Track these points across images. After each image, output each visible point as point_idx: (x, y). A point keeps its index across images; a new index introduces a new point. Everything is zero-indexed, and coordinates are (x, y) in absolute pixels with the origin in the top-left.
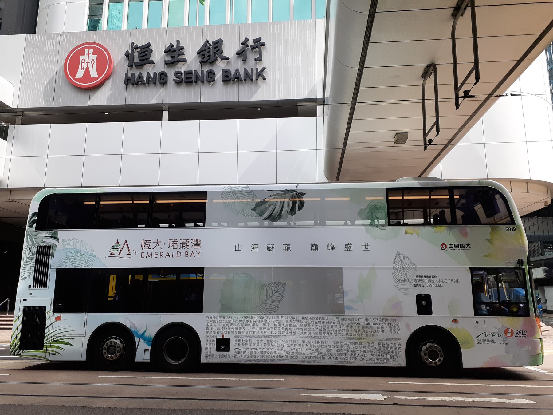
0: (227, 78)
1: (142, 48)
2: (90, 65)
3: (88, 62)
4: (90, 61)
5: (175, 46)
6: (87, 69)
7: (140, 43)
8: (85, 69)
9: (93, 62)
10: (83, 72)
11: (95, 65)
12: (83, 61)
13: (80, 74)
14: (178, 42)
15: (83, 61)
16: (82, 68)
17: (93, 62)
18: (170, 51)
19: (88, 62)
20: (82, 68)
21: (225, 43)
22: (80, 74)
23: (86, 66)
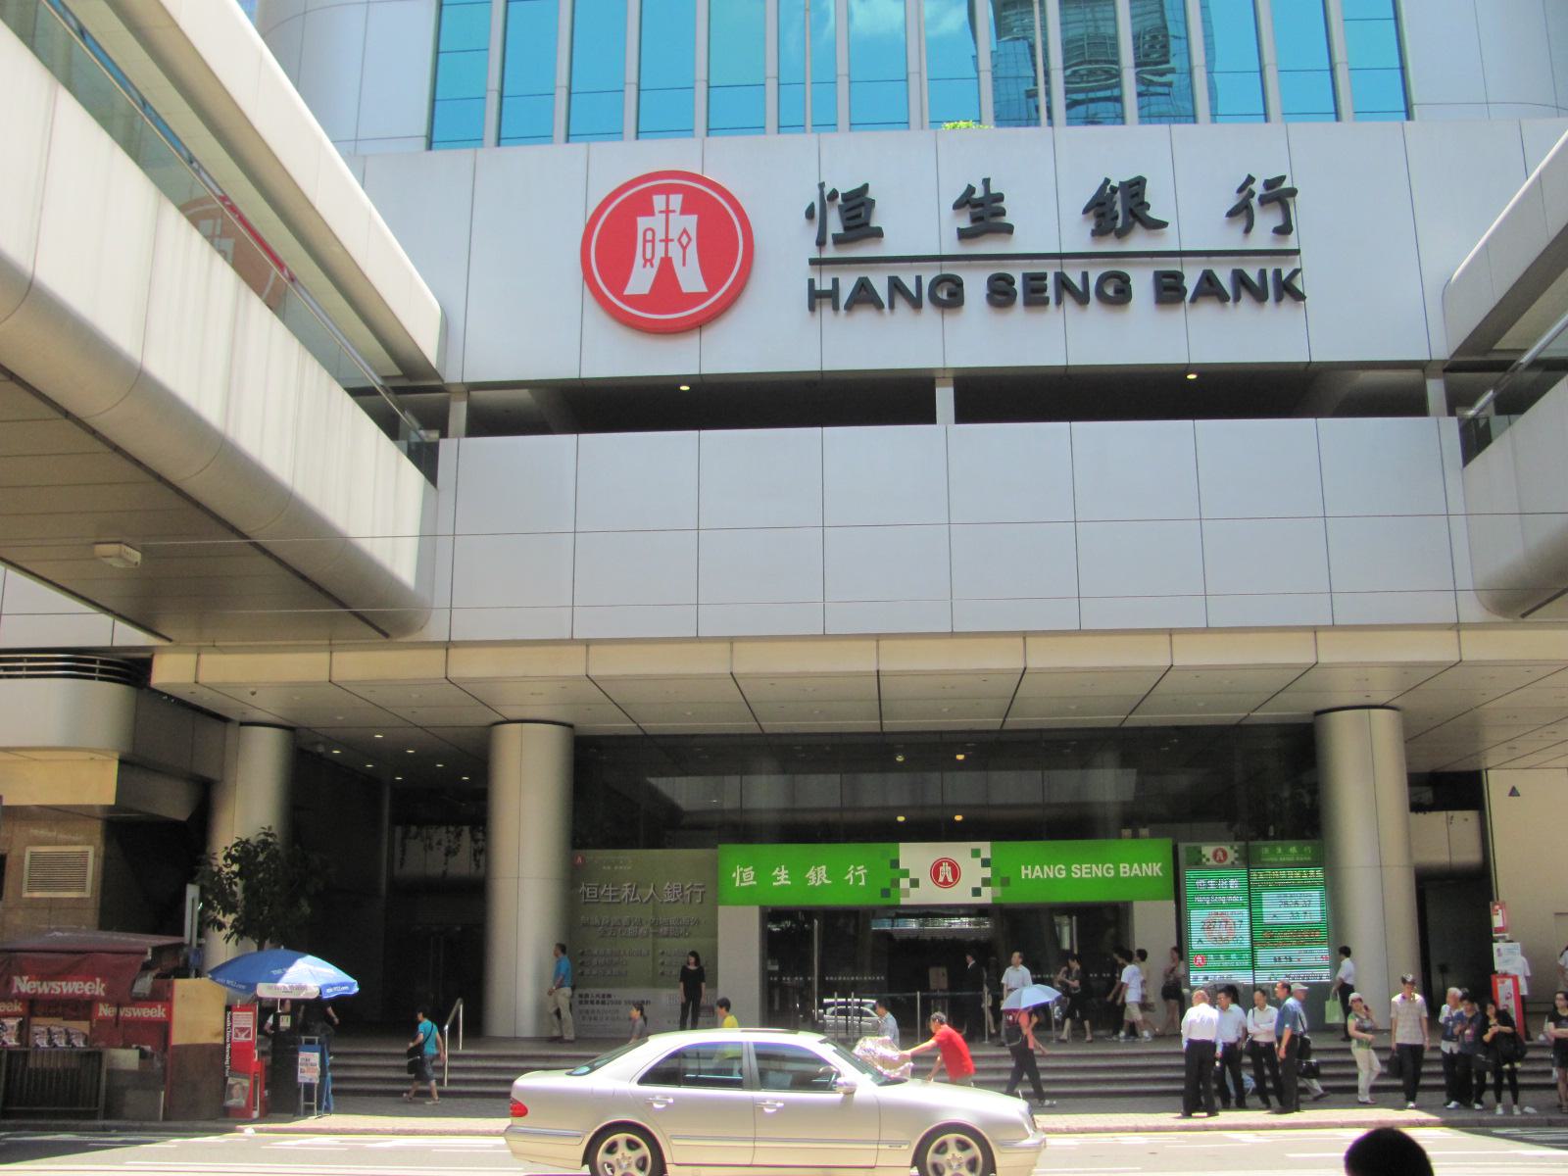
0: (1169, 290)
1: (847, 197)
2: (675, 252)
3: (667, 240)
4: (674, 234)
5: (979, 194)
6: (667, 262)
7: (844, 188)
8: (657, 262)
9: (685, 240)
10: (651, 273)
11: (693, 249)
12: (649, 236)
13: (641, 281)
14: (986, 182)
15: (649, 236)
16: (647, 261)
17: (685, 240)
18: (965, 201)
19: (667, 240)
20: (647, 261)
21: (1148, 185)
22: (641, 281)
23: (660, 253)
